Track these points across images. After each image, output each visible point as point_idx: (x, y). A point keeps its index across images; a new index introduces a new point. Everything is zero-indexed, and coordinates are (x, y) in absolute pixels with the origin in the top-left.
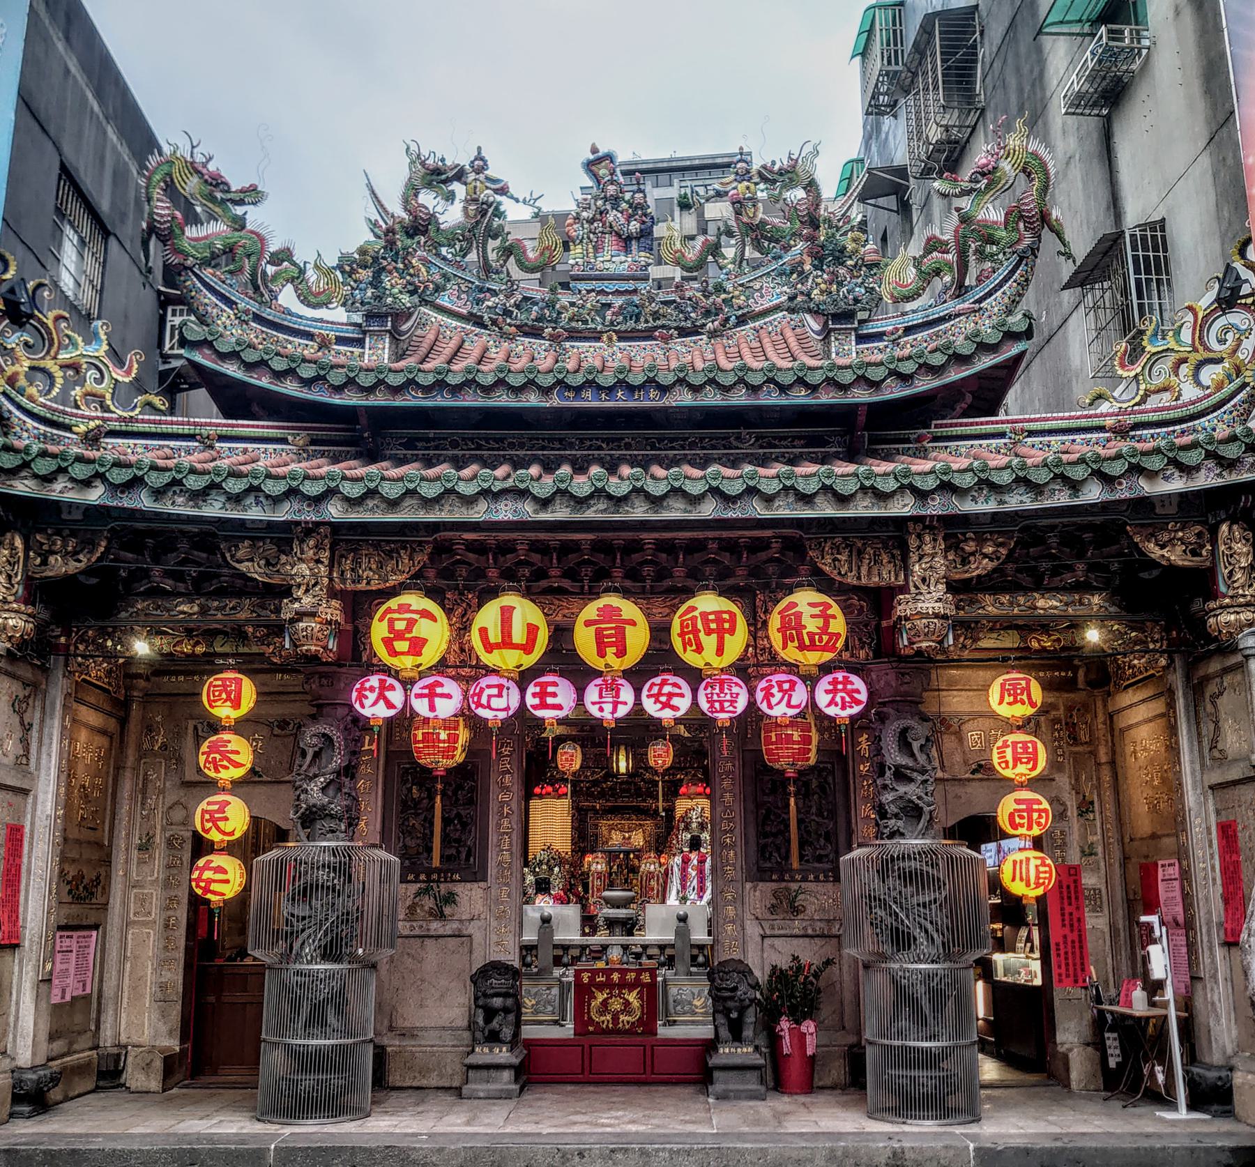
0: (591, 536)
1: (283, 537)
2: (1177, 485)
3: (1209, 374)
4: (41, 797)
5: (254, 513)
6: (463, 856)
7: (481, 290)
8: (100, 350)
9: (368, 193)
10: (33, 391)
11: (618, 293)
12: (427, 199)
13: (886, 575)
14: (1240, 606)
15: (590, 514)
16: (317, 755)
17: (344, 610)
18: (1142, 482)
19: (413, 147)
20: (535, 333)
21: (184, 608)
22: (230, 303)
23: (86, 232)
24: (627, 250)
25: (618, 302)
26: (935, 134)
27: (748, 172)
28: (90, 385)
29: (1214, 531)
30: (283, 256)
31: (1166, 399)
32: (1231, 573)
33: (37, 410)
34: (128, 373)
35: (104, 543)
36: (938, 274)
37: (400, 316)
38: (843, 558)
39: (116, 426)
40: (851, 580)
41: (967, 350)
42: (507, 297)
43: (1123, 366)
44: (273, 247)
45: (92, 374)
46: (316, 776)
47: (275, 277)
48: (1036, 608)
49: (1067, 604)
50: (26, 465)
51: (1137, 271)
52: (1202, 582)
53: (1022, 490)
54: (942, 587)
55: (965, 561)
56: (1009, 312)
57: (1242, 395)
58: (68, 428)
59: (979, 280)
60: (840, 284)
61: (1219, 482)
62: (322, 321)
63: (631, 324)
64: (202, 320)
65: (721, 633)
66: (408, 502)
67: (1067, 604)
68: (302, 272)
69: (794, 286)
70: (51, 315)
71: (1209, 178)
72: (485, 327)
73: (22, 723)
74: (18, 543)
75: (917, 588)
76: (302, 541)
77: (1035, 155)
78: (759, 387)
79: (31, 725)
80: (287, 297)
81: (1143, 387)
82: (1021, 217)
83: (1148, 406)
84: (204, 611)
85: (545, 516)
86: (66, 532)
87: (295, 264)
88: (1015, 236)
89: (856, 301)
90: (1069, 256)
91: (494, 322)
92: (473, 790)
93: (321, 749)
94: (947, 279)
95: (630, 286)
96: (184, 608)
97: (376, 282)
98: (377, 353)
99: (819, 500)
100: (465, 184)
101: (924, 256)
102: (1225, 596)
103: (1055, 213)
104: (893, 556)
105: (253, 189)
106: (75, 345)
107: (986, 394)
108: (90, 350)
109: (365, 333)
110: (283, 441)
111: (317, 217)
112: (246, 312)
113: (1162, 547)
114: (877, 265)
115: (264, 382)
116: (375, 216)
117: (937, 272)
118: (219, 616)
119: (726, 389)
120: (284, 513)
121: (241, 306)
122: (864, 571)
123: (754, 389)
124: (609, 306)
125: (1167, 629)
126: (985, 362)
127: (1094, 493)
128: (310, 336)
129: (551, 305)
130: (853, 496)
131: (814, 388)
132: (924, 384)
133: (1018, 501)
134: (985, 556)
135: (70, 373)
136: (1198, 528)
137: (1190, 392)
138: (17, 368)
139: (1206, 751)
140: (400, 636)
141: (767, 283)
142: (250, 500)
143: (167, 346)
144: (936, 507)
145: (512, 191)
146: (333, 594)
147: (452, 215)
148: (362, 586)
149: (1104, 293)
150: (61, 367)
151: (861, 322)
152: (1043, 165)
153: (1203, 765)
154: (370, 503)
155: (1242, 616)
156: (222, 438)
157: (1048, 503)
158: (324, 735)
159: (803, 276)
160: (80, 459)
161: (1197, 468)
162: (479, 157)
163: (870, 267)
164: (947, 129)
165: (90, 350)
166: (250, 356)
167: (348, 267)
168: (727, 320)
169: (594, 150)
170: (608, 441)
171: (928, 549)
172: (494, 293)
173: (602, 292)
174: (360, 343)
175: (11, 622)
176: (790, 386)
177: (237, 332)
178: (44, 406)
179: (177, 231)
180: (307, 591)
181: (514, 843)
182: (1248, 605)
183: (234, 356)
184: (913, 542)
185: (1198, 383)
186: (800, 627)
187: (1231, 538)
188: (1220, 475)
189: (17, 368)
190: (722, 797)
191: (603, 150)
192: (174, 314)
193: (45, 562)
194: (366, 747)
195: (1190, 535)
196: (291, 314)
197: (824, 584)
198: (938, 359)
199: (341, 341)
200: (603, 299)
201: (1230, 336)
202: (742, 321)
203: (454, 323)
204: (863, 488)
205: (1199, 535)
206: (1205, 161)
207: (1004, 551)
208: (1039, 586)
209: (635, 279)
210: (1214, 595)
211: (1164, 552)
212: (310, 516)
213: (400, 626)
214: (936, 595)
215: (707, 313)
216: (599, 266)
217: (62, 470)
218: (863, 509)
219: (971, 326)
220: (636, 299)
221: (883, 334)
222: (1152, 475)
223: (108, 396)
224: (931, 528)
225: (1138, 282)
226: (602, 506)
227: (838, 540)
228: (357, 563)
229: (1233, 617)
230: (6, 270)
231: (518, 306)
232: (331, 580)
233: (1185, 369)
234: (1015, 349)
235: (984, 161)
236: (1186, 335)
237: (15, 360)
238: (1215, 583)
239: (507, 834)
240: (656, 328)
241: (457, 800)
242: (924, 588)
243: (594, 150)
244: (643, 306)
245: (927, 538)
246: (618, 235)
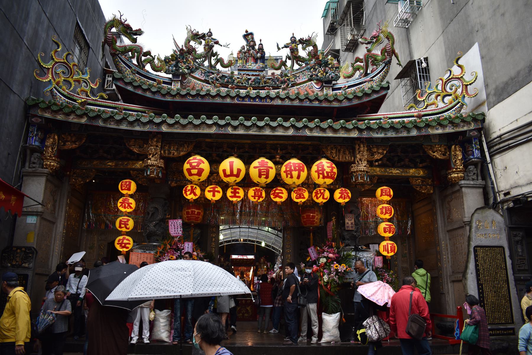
0: (249, 142)
1: (145, 137)
2: (440, 131)
3: (447, 99)
4: (58, 225)
5: (137, 128)
7: (209, 72)
8: (87, 77)
9: (173, 41)
10: (64, 87)
11: (253, 75)
12: (192, 43)
13: (348, 158)
14: (459, 171)
15: (251, 132)
16: (153, 214)
17: (165, 164)
18: (429, 130)
19: (189, 27)
20: (226, 86)
21: (110, 164)
22: (130, 67)
23: (83, 45)
24: (256, 62)
25: (253, 78)
26: (349, 37)
27: (295, 41)
28: (83, 88)
29: (450, 148)
30: (148, 53)
31: (433, 107)
32: (455, 161)
33: (65, 93)
34: (96, 85)
35: (85, 139)
36: (358, 70)
37: (184, 75)
38: (334, 152)
39: (91, 102)
40: (336, 158)
41: (369, 92)
42: (218, 75)
43: (419, 97)
44: (145, 51)
45: (84, 84)
46: (153, 221)
47: (145, 60)
48: (392, 173)
49: (402, 172)
50: (61, 110)
51: (420, 72)
53: (392, 131)
54: (366, 162)
55: (373, 155)
56: (382, 81)
57: (458, 105)
58: (75, 101)
59: (372, 72)
60: (327, 73)
61: (453, 131)
62: (158, 76)
63: (257, 85)
64: (120, 71)
66: (189, 126)
67: (402, 172)
68: (154, 59)
69: (312, 72)
70: (72, 64)
71: (443, 44)
72: (210, 84)
73: (54, 199)
74: (56, 137)
75: (358, 162)
76: (152, 139)
77: (390, 33)
78: (303, 100)
79: (56, 200)
80: (148, 67)
81: (426, 103)
82: (386, 52)
83: (428, 109)
84: (116, 165)
86: (72, 135)
87: (151, 56)
88: (384, 57)
89: (332, 77)
90: (400, 65)
91: (213, 82)
93: (154, 213)
94: (362, 71)
95: (257, 73)
96: (110, 164)
97: (176, 66)
98: (176, 86)
99: (328, 131)
100: (205, 40)
101: (355, 63)
102: (454, 168)
103: (396, 51)
104: (350, 152)
105: (140, 30)
106: (79, 74)
107: (375, 105)
108: (84, 77)
109: (172, 81)
110: (145, 112)
111: (159, 42)
112: (135, 70)
113: (434, 152)
114: (338, 68)
115: (140, 92)
116: (175, 49)
117: (358, 69)
118: (122, 167)
119: (292, 100)
120: (147, 129)
121: (133, 68)
122: (341, 157)
123: (301, 100)
124: (250, 79)
125: (432, 181)
126: (375, 96)
127: (414, 133)
128: (154, 80)
129: (231, 78)
130: (339, 130)
131: (320, 101)
132: (356, 102)
133: (391, 134)
134: (379, 153)
135: (77, 83)
136: (445, 147)
137: (441, 105)
138: (60, 79)
139: (446, 219)
141: (301, 74)
142: (136, 124)
143: (106, 86)
144: (365, 135)
145: (220, 43)
146: (162, 157)
147: (200, 49)
148: (171, 155)
149: (406, 81)
150: (74, 81)
151: (334, 84)
152: (393, 36)
153: (445, 224)
154: (176, 126)
155: (459, 175)
156: (125, 109)
157: (400, 135)
158: (156, 208)
159: (315, 70)
160: (79, 108)
161: (446, 126)
162: (210, 32)
163: (336, 68)
164: (354, 36)
165: (84, 77)
166: (135, 84)
167: (167, 61)
168: (288, 85)
169: (247, 32)
171: (362, 149)
172: (213, 73)
173: (248, 75)
174: (171, 84)
175: (52, 164)
176: (313, 100)
177: (132, 76)
178: (68, 93)
179: (114, 42)
180: (153, 156)
182: (460, 171)
183: (130, 84)
184: (357, 147)
185: (443, 102)
187: (456, 150)
188: (453, 129)
189: (60, 79)
191: (249, 32)
192: (108, 77)
193: (64, 144)
196: (149, 72)
197: (328, 159)
198: (360, 94)
199: (164, 83)
200: (249, 77)
201: (454, 88)
202: (293, 86)
203: (200, 82)
204: (342, 127)
205: (445, 149)
206: (441, 38)
207: (385, 152)
208: (394, 166)
209: (259, 71)
210: (451, 168)
211: (435, 154)
212: (154, 129)
214: (364, 165)
215: (283, 82)
216: (247, 66)
217: (73, 112)
218: (342, 134)
219: (369, 85)
220: (259, 78)
221: (341, 88)
222: (433, 127)
223: (89, 92)
224: (363, 142)
225: (420, 76)
226: (255, 130)
227: (332, 146)
228: (170, 148)
229: (456, 175)
230: (58, 48)
231: (220, 78)
232: (161, 152)
233: (439, 98)
234: (384, 93)
235: (374, 34)
236: (440, 87)
237: (59, 77)
238: (450, 164)
240: (265, 86)
242: (360, 162)
243: (247, 32)
244: (261, 79)
245: (362, 146)
246: (254, 57)
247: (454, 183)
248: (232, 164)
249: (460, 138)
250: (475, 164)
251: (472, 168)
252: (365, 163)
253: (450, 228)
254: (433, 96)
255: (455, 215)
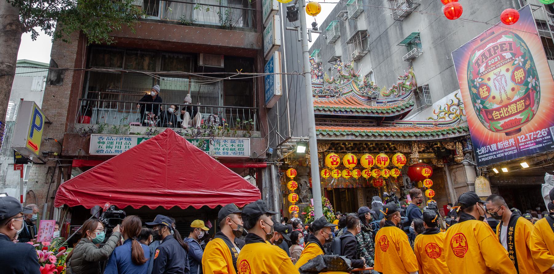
3: (451, 116)
29: (455, 143)
31: (443, 120)
52: (454, 152)
59: (403, 94)
63: (320, 94)
65: (385, 161)
85: (357, 139)
140: (335, 161)
144: (419, 139)
170: (333, 120)
186: (401, 160)
195: (452, 144)
213: (335, 159)
215: (337, 93)
233: (447, 115)
247: (458, 164)
248: (365, 158)
249: (462, 139)
250: (470, 153)
251: (468, 154)
252: (417, 154)
253: (456, 187)
254: (443, 113)
255: (460, 179)
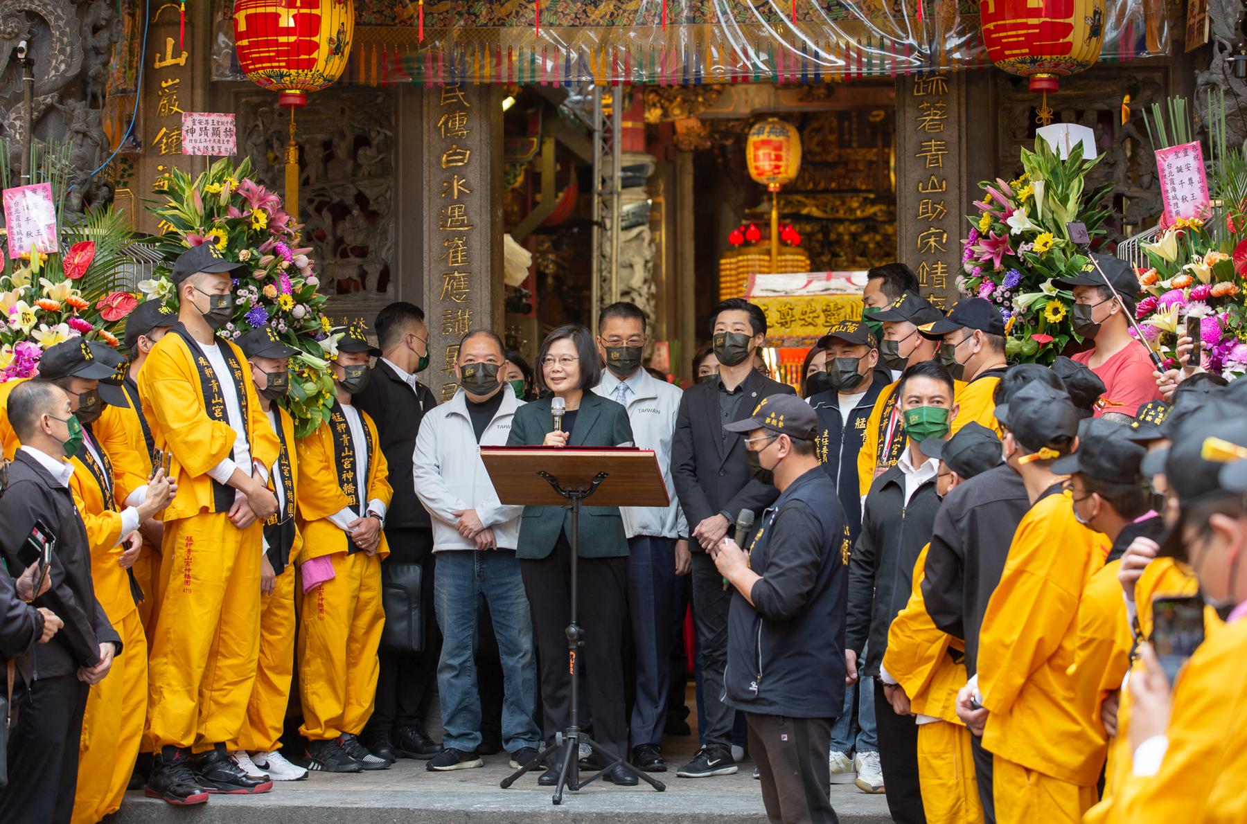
6: (372, 281)
92: (389, 145)
181: (476, 253)
190: (920, 148)
194: (169, 61)
239: (460, 235)
241: (358, 166)
